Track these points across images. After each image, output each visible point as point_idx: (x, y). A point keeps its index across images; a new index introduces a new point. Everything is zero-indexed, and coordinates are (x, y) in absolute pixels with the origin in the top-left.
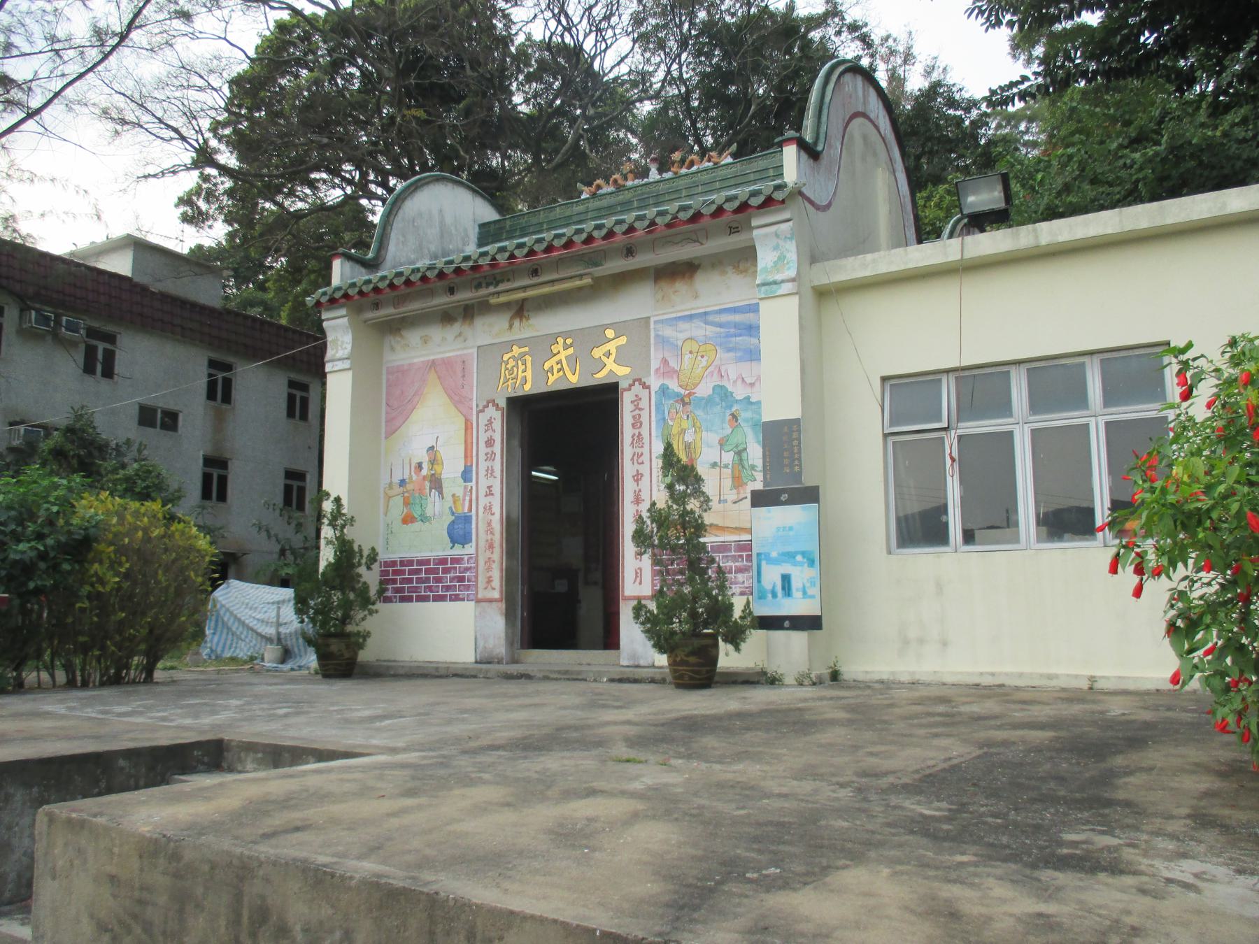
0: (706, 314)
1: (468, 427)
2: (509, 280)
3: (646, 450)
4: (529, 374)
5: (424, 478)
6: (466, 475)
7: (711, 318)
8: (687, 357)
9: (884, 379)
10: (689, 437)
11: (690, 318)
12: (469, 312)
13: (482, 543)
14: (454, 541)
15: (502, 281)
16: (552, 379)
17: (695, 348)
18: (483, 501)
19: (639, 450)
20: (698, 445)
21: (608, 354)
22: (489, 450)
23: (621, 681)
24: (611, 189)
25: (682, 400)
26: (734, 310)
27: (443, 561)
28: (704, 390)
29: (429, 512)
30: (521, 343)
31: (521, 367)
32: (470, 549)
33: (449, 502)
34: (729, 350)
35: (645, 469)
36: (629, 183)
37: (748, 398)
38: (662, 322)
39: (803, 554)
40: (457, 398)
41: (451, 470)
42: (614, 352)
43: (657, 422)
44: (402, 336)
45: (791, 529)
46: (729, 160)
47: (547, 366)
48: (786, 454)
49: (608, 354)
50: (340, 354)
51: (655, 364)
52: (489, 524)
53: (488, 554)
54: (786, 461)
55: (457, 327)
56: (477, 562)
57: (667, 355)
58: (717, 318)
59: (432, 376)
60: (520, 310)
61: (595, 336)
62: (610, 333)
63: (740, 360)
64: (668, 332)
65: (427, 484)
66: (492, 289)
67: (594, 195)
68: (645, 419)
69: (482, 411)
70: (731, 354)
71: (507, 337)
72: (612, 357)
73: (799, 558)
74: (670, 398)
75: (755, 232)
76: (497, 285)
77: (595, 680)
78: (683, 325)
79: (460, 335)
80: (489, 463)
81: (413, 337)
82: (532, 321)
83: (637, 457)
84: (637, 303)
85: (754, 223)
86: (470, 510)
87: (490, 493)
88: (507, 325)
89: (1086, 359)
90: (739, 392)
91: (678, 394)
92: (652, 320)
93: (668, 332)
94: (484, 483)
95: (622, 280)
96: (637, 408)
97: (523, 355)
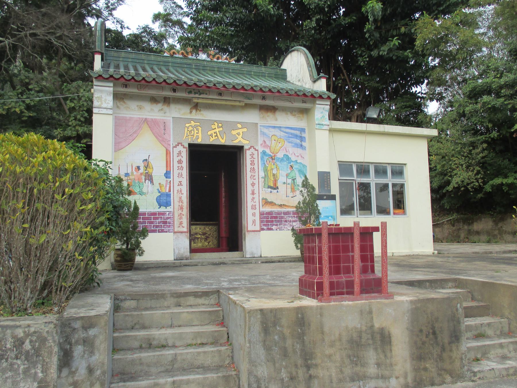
0: (280, 127)
1: (168, 153)
2: (206, 94)
3: (256, 174)
4: (200, 135)
5: (141, 174)
6: (167, 175)
7: (283, 129)
8: (273, 142)
9: (338, 161)
10: (275, 172)
11: (274, 127)
12: (167, 101)
13: (176, 207)
14: (160, 206)
15: (203, 94)
16: (212, 139)
17: (276, 139)
18: (177, 188)
19: (254, 174)
20: (278, 175)
21: (238, 134)
22: (180, 165)
23: (266, 262)
24: (181, 56)
25: (272, 157)
26: (291, 128)
27: (154, 214)
28: (280, 155)
29: (145, 190)
30: (195, 120)
31: (196, 131)
32: (169, 209)
33: (157, 186)
34: (289, 142)
35: (256, 182)
36: (190, 57)
37: (296, 161)
38: (263, 126)
39: (331, 216)
40: (160, 139)
41: (158, 170)
42: (241, 133)
43: (262, 164)
44: (125, 102)
45: (327, 208)
46: (234, 62)
47: (209, 133)
48: (326, 183)
49: (238, 134)
50: (104, 105)
51: (260, 142)
52: (180, 198)
53: (180, 211)
54: (326, 186)
55: (160, 106)
56: (173, 215)
57: (265, 139)
58: (283, 129)
59: (145, 127)
60: (196, 106)
61: (233, 125)
62: (239, 126)
63: (294, 147)
64: (265, 130)
65: (143, 177)
66: (197, 96)
67: (172, 56)
68: (256, 162)
69: (175, 147)
70: (290, 144)
71: (189, 116)
72: (241, 135)
73: (330, 218)
74: (266, 156)
75: (317, 106)
76: (200, 94)
77: (255, 263)
78: (271, 129)
79: (162, 110)
80: (180, 171)
81: (133, 105)
82: (202, 112)
83: (253, 177)
84: (252, 117)
85: (318, 102)
86: (170, 191)
87: (180, 184)
88: (189, 111)
89: (388, 165)
90: (293, 158)
91: (270, 155)
92: (259, 125)
93: (265, 130)
94: (177, 180)
95: (247, 106)
96: (252, 157)
97: (196, 126)
